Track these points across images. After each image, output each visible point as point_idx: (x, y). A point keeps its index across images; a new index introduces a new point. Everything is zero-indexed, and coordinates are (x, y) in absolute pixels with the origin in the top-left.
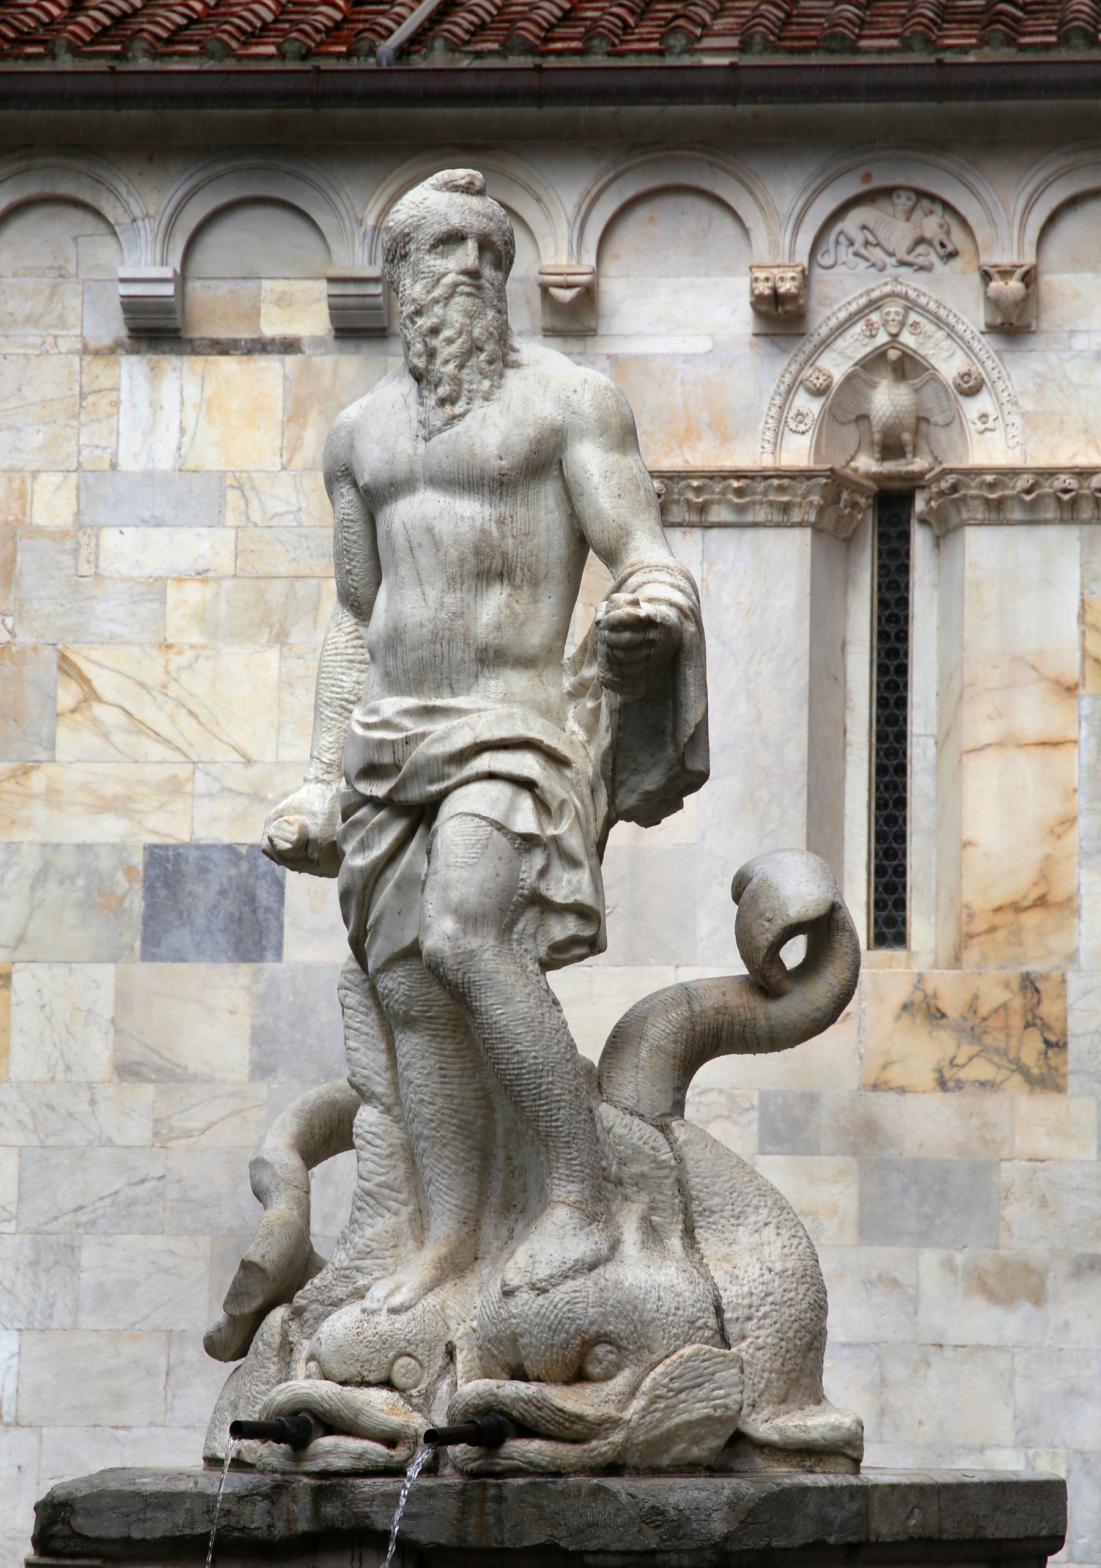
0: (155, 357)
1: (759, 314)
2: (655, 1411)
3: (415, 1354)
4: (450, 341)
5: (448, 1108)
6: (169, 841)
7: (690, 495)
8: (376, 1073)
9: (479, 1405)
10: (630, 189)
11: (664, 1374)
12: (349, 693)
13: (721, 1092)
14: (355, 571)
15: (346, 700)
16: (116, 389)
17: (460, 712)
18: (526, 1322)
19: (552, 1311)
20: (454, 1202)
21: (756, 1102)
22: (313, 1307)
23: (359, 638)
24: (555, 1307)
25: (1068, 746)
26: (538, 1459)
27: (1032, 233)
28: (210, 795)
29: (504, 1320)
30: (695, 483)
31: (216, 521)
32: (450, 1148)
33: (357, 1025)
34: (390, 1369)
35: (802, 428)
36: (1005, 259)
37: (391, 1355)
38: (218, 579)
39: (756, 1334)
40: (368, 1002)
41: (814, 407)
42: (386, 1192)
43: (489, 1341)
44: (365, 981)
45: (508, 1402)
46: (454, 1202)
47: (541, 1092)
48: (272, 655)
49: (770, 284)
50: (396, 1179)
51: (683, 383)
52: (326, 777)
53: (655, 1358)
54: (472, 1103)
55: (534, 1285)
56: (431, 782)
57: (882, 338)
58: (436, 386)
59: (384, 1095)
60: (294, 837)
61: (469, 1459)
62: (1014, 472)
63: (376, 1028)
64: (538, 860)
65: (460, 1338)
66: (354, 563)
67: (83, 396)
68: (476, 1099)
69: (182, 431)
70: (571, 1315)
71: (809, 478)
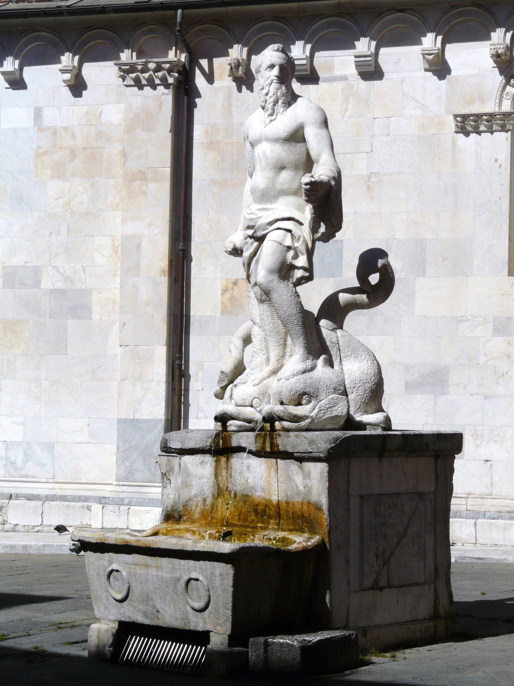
2: (320, 414)
4: (271, 97)
13: (481, 317)
14: (251, 167)
21: (492, 320)
34: (252, 402)
35: (508, 97)
37: (253, 397)
39: (357, 391)
42: (259, 351)
49: (495, 50)
51: (469, 85)
53: (322, 398)
56: (263, 230)
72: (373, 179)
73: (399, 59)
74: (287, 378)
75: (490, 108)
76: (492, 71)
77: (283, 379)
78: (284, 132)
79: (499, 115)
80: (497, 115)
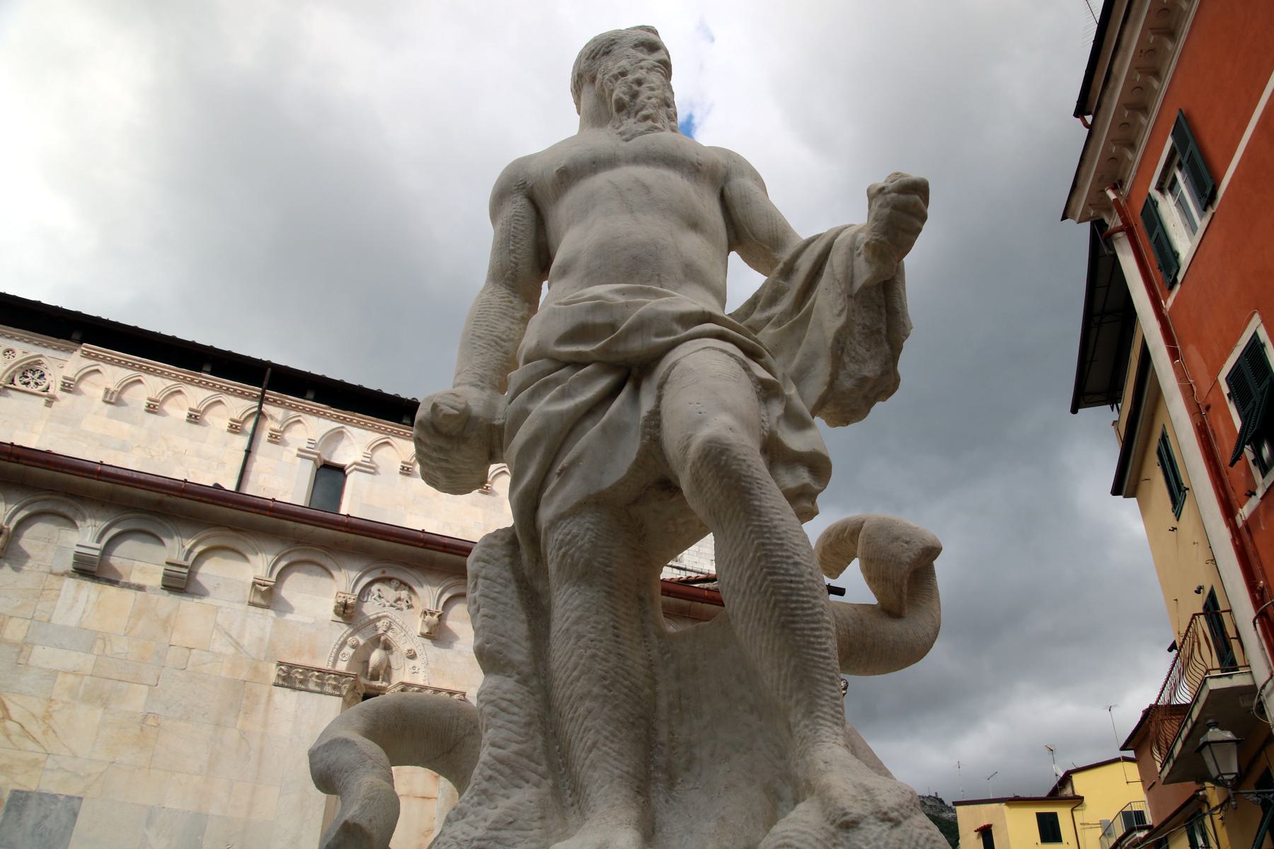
0: (81, 581)
1: (337, 612)
4: (652, 89)
6: (24, 789)
7: (298, 675)
8: (515, 642)
10: (295, 557)
12: (503, 333)
15: (499, 337)
16: (60, 590)
20: (625, 769)
23: (511, 302)
24: (917, 843)
25: (433, 800)
27: (441, 604)
28: (52, 770)
30: (300, 670)
31: (90, 650)
33: (495, 595)
35: (344, 659)
36: (432, 609)
38: (83, 675)
40: (508, 575)
41: (351, 651)
42: (525, 761)
44: (505, 556)
46: (625, 769)
47: (815, 614)
48: (100, 711)
50: (535, 749)
52: (479, 383)
54: (642, 669)
55: (885, 813)
56: (658, 335)
57: (381, 631)
58: (637, 113)
59: (523, 663)
60: (462, 406)
64: (777, 409)
66: (518, 246)
67: (43, 589)
69: (84, 612)
71: (347, 677)
72: (151, 721)
73: (218, 584)
74: (894, 815)
75: (324, 664)
76: (331, 625)
77: (872, 819)
78: (698, 154)
80: (332, 674)
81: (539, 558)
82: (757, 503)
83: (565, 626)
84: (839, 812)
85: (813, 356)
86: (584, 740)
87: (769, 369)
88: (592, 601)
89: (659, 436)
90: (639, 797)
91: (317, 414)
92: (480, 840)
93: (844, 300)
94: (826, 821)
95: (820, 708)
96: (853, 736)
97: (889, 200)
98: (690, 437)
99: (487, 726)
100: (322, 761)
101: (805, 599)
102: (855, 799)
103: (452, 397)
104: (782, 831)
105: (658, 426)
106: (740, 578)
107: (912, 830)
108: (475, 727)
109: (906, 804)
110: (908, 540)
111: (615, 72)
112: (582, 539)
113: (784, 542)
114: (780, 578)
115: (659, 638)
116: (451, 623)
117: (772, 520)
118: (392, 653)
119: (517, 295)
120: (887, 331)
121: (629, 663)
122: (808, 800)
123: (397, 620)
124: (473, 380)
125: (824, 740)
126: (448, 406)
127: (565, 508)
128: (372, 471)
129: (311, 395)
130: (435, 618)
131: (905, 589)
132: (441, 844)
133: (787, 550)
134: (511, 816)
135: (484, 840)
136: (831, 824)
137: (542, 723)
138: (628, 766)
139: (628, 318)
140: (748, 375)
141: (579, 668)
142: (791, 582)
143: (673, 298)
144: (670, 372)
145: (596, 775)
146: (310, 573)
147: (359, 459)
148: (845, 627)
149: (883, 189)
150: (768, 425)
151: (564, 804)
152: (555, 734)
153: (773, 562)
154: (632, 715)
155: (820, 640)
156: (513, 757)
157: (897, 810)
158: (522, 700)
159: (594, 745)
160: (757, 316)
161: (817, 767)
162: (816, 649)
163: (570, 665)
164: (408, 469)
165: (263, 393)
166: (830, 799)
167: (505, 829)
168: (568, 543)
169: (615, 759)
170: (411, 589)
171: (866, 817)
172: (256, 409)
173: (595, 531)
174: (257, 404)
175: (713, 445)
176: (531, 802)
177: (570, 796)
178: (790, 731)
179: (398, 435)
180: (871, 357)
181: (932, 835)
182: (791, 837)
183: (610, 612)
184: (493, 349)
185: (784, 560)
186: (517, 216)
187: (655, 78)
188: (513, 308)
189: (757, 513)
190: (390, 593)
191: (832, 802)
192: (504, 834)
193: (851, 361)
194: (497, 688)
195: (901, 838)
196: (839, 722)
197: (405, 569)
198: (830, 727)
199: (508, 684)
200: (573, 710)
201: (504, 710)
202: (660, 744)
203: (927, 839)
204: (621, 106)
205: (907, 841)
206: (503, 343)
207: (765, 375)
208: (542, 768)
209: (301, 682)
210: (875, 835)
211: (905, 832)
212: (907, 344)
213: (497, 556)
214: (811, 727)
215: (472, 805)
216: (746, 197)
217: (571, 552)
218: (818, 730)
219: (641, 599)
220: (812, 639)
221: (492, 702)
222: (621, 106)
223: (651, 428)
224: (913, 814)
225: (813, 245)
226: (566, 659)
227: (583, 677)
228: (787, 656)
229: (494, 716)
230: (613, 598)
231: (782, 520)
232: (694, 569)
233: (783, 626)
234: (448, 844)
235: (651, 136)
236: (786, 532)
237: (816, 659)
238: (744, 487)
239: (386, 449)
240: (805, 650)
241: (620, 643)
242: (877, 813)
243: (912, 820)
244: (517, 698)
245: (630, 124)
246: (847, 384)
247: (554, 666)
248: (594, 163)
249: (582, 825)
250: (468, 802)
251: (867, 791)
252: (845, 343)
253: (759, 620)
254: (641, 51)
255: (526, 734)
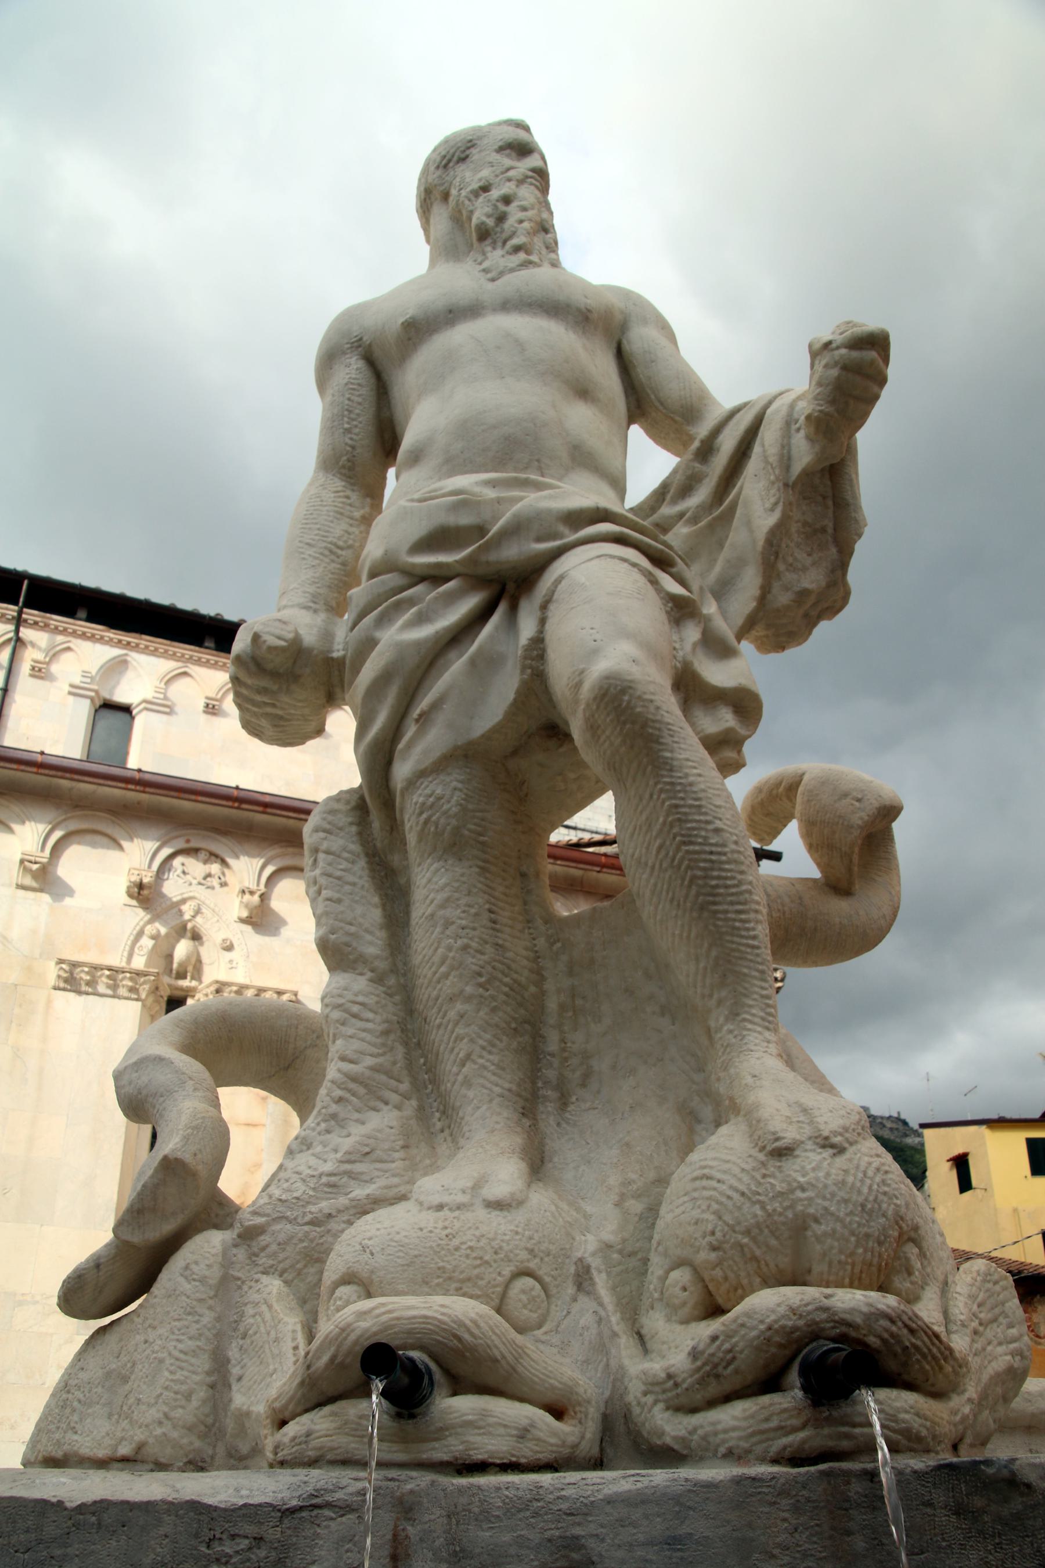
3: (541, 1273)
4: (524, 209)
5: (500, 962)
7: (83, 976)
8: (367, 931)
9: (795, 1329)
10: (74, 825)
11: (972, 1297)
12: (339, 538)
14: (357, 430)
15: (335, 545)
17: (559, 487)
18: (824, 1198)
19: (862, 1181)
20: (507, 1085)
22: (277, 1227)
23: (348, 497)
24: (865, 1173)
26: (916, 1424)
29: (781, 1194)
30: (86, 969)
32: (501, 1014)
33: (339, 873)
34: (504, 1296)
35: (142, 953)
36: (254, 887)
37: (507, 1272)
40: (355, 847)
41: (151, 943)
42: (383, 1078)
43: (747, 1232)
44: (351, 824)
45: (859, 1320)
46: (507, 1085)
47: (741, 893)
50: (394, 1063)
54: (525, 962)
55: (827, 1138)
56: (539, 539)
58: (505, 242)
59: (377, 957)
60: (291, 636)
61: (780, 1428)
62: (247, 987)
63: (366, 878)
64: (692, 633)
65: (593, 1254)
66: (355, 423)
68: (527, 959)
70: (886, 1189)
71: (146, 975)
74: (837, 1140)
75: (116, 960)
77: (809, 1145)
79: (130, 973)
81: (394, 825)
82: (668, 755)
83: (429, 911)
84: (772, 1137)
85: (737, 565)
86: (456, 1051)
87: (682, 581)
88: (464, 879)
89: (543, 670)
90: (524, 1120)
91: (92, 638)
92: (330, 1175)
93: (779, 490)
94: (754, 1147)
95: (747, 1009)
96: (789, 1043)
97: (837, 358)
98: (582, 672)
99: (334, 1035)
100: (130, 1083)
101: (729, 874)
102: (789, 1120)
103: (277, 624)
104: (701, 1160)
105: (542, 656)
106: (647, 848)
107: (860, 1158)
108: (318, 1037)
109: (853, 1126)
110: (860, 796)
111: (475, 186)
112: (449, 802)
113: (703, 803)
114: (697, 848)
115: (546, 922)
116: (276, 904)
117: (687, 775)
118: (202, 944)
119: (355, 488)
120: (835, 529)
121: (510, 954)
122: (731, 1122)
123: (207, 902)
124: (302, 600)
125: (753, 1048)
126: (273, 635)
127: (427, 762)
128: (167, 710)
129: (82, 613)
130: (256, 898)
131: (856, 858)
132: (282, 1181)
133: (706, 814)
134: (367, 1145)
135: (335, 1175)
136: (760, 1151)
137: (402, 1031)
138: (510, 1083)
139: (500, 518)
140: (656, 590)
141: (448, 962)
142: (711, 853)
143: (557, 490)
144: (556, 587)
145: (471, 1094)
146: (94, 845)
147: (149, 695)
148: (780, 907)
149: (830, 343)
150: (681, 653)
151: (432, 1130)
152: (419, 1044)
153: (689, 829)
154: (514, 1019)
155: (747, 925)
156: (368, 1073)
157: (841, 1135)
158: (377, 1003)
159: (468, 1057)
160: (667, 510)
161: (744, 1082)
162: (742, 937)
163: (436, 959)
164: (214, 706)
165: (20, 613)
166: (759, 1121)
167: (361, 1162)
168: (431, 806)
169: (494, 1074)
170: (224, 862)
171: (802, 1142)
172: (12, 635)
173: (465, 791)
174: (12, 627)
175: (611, 681)
176: (392, 1128)
177: (439, 1120)
178: (710, 1038)
179: (198, 662)
180: (814, 564)
181: (883, 1164)
182: (711, 1167)
183: (485, 893)
184: (327, 560)
185: (703, 825)
186: (352, 384)
187: (527, 194)
188: (350, 505)
189: (668, 767)
190: (196, 867)
191: (762, 1125)
192: (358, 1167)
193: (787, 570)
194: (346, 989)
195: (845, 1168)
196: (771, 1026)
197: (213, 835)
198: (760, 1033)
199: (359, 983)
200: (441, 1014)
201: (355, 1016)
202: (549, 1055)
203: (878, 1170)
204: (484, 234)
205: (852, 1172)
206: (340, 552)
207: (676, 589)
208: (405, 1086)
209: (88, 984)
210: (813, 1165)
211: (850, 1160)
212: (859, 547)
213: (341, 824)
214: (736, 1032)
215: (319, 1134)
216: (650, 353)
217: (434, 818)
218: (744, 1037)
219: (523, 875)
220: (737, 924)
221: (338, 1006)
222: (484, 234)
223: (533, 659)
224: (860, 1139)
225: (738, 416)
226: (431, 952)
227: (453, 973)
228: (706, 945)
229: (343, 1024)
230: (488, 875)
231: (700, 775)
232: (588, 828)
233: (702, 908)
234: (291, 1181)
235: (524, 273)
236: (704, 791)
237: (743, 948)
238: (652, 734)
239: (185, 681)
240: (728, 938)
241: (498, 931)
242: (816, 1137)
243: (859, 1146)
244: (371, 1000)
245: (496, 257)
246: (782, 598)
247: (416, 960)
248: (450, 311)
249: (455, 1155)
250: (314, 1129)
251: (805, 1111)
252: (779, 546)
253: (672, 901)
254: (508, 156)
255: (384, 1045)
